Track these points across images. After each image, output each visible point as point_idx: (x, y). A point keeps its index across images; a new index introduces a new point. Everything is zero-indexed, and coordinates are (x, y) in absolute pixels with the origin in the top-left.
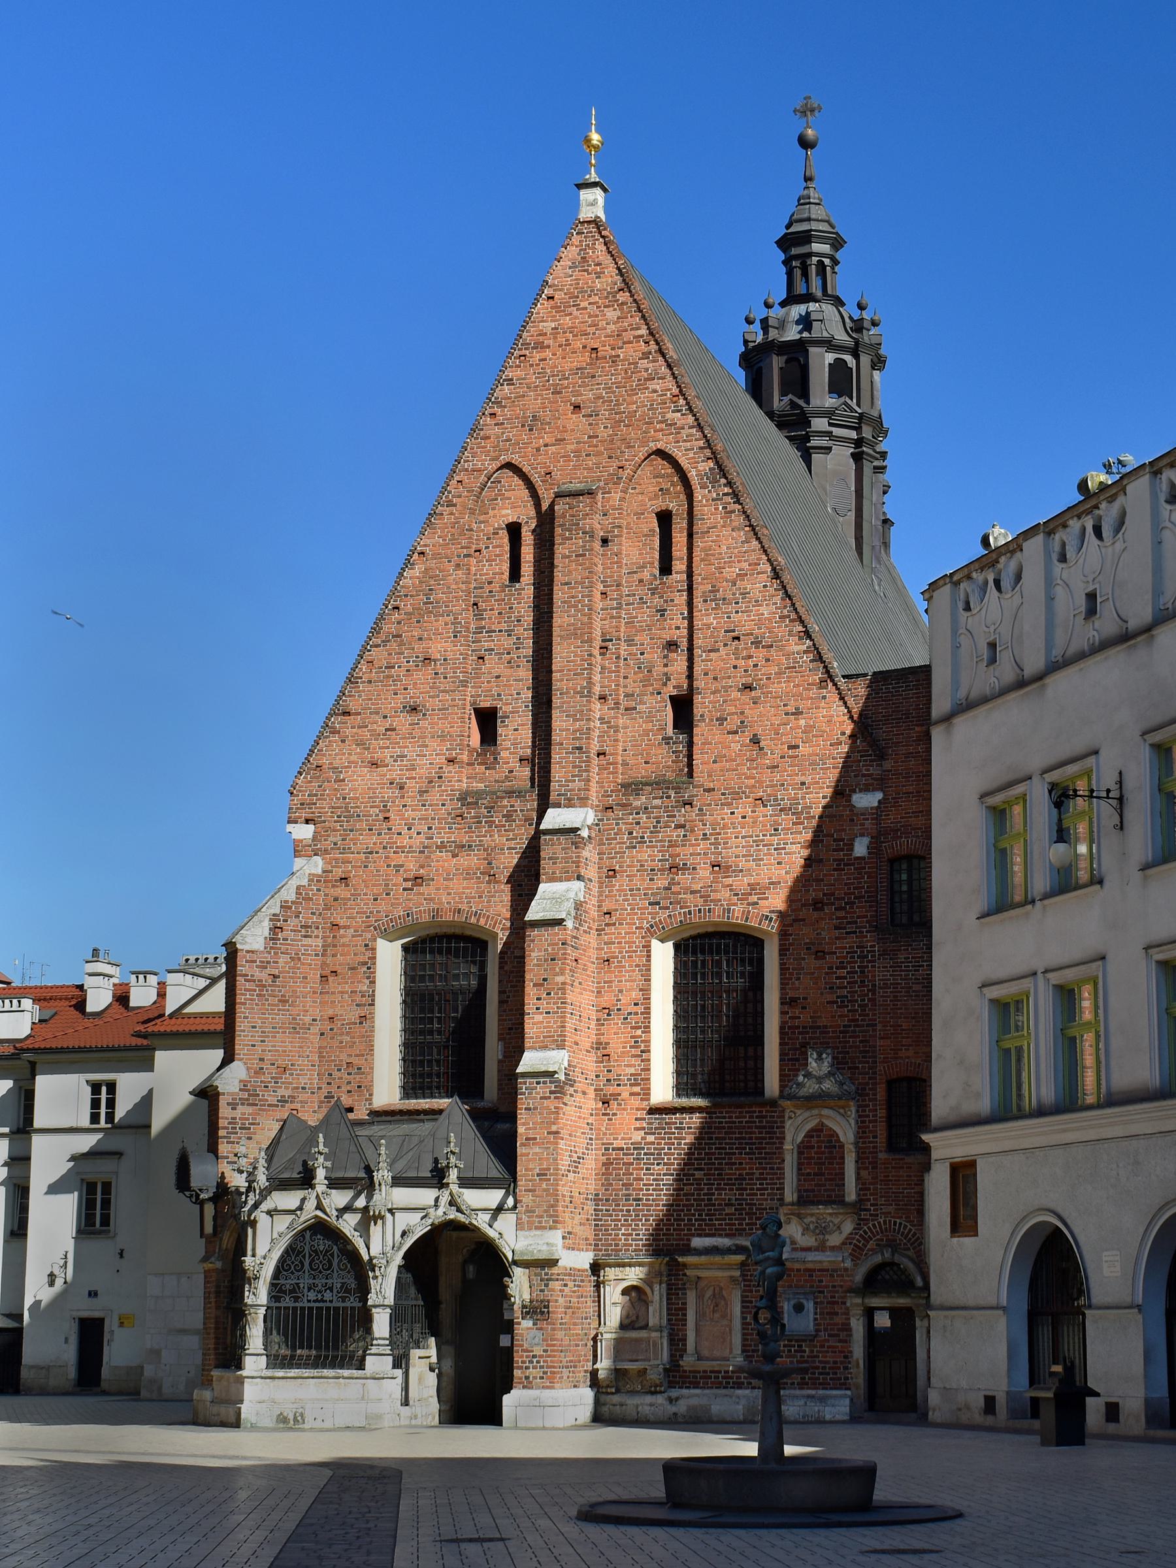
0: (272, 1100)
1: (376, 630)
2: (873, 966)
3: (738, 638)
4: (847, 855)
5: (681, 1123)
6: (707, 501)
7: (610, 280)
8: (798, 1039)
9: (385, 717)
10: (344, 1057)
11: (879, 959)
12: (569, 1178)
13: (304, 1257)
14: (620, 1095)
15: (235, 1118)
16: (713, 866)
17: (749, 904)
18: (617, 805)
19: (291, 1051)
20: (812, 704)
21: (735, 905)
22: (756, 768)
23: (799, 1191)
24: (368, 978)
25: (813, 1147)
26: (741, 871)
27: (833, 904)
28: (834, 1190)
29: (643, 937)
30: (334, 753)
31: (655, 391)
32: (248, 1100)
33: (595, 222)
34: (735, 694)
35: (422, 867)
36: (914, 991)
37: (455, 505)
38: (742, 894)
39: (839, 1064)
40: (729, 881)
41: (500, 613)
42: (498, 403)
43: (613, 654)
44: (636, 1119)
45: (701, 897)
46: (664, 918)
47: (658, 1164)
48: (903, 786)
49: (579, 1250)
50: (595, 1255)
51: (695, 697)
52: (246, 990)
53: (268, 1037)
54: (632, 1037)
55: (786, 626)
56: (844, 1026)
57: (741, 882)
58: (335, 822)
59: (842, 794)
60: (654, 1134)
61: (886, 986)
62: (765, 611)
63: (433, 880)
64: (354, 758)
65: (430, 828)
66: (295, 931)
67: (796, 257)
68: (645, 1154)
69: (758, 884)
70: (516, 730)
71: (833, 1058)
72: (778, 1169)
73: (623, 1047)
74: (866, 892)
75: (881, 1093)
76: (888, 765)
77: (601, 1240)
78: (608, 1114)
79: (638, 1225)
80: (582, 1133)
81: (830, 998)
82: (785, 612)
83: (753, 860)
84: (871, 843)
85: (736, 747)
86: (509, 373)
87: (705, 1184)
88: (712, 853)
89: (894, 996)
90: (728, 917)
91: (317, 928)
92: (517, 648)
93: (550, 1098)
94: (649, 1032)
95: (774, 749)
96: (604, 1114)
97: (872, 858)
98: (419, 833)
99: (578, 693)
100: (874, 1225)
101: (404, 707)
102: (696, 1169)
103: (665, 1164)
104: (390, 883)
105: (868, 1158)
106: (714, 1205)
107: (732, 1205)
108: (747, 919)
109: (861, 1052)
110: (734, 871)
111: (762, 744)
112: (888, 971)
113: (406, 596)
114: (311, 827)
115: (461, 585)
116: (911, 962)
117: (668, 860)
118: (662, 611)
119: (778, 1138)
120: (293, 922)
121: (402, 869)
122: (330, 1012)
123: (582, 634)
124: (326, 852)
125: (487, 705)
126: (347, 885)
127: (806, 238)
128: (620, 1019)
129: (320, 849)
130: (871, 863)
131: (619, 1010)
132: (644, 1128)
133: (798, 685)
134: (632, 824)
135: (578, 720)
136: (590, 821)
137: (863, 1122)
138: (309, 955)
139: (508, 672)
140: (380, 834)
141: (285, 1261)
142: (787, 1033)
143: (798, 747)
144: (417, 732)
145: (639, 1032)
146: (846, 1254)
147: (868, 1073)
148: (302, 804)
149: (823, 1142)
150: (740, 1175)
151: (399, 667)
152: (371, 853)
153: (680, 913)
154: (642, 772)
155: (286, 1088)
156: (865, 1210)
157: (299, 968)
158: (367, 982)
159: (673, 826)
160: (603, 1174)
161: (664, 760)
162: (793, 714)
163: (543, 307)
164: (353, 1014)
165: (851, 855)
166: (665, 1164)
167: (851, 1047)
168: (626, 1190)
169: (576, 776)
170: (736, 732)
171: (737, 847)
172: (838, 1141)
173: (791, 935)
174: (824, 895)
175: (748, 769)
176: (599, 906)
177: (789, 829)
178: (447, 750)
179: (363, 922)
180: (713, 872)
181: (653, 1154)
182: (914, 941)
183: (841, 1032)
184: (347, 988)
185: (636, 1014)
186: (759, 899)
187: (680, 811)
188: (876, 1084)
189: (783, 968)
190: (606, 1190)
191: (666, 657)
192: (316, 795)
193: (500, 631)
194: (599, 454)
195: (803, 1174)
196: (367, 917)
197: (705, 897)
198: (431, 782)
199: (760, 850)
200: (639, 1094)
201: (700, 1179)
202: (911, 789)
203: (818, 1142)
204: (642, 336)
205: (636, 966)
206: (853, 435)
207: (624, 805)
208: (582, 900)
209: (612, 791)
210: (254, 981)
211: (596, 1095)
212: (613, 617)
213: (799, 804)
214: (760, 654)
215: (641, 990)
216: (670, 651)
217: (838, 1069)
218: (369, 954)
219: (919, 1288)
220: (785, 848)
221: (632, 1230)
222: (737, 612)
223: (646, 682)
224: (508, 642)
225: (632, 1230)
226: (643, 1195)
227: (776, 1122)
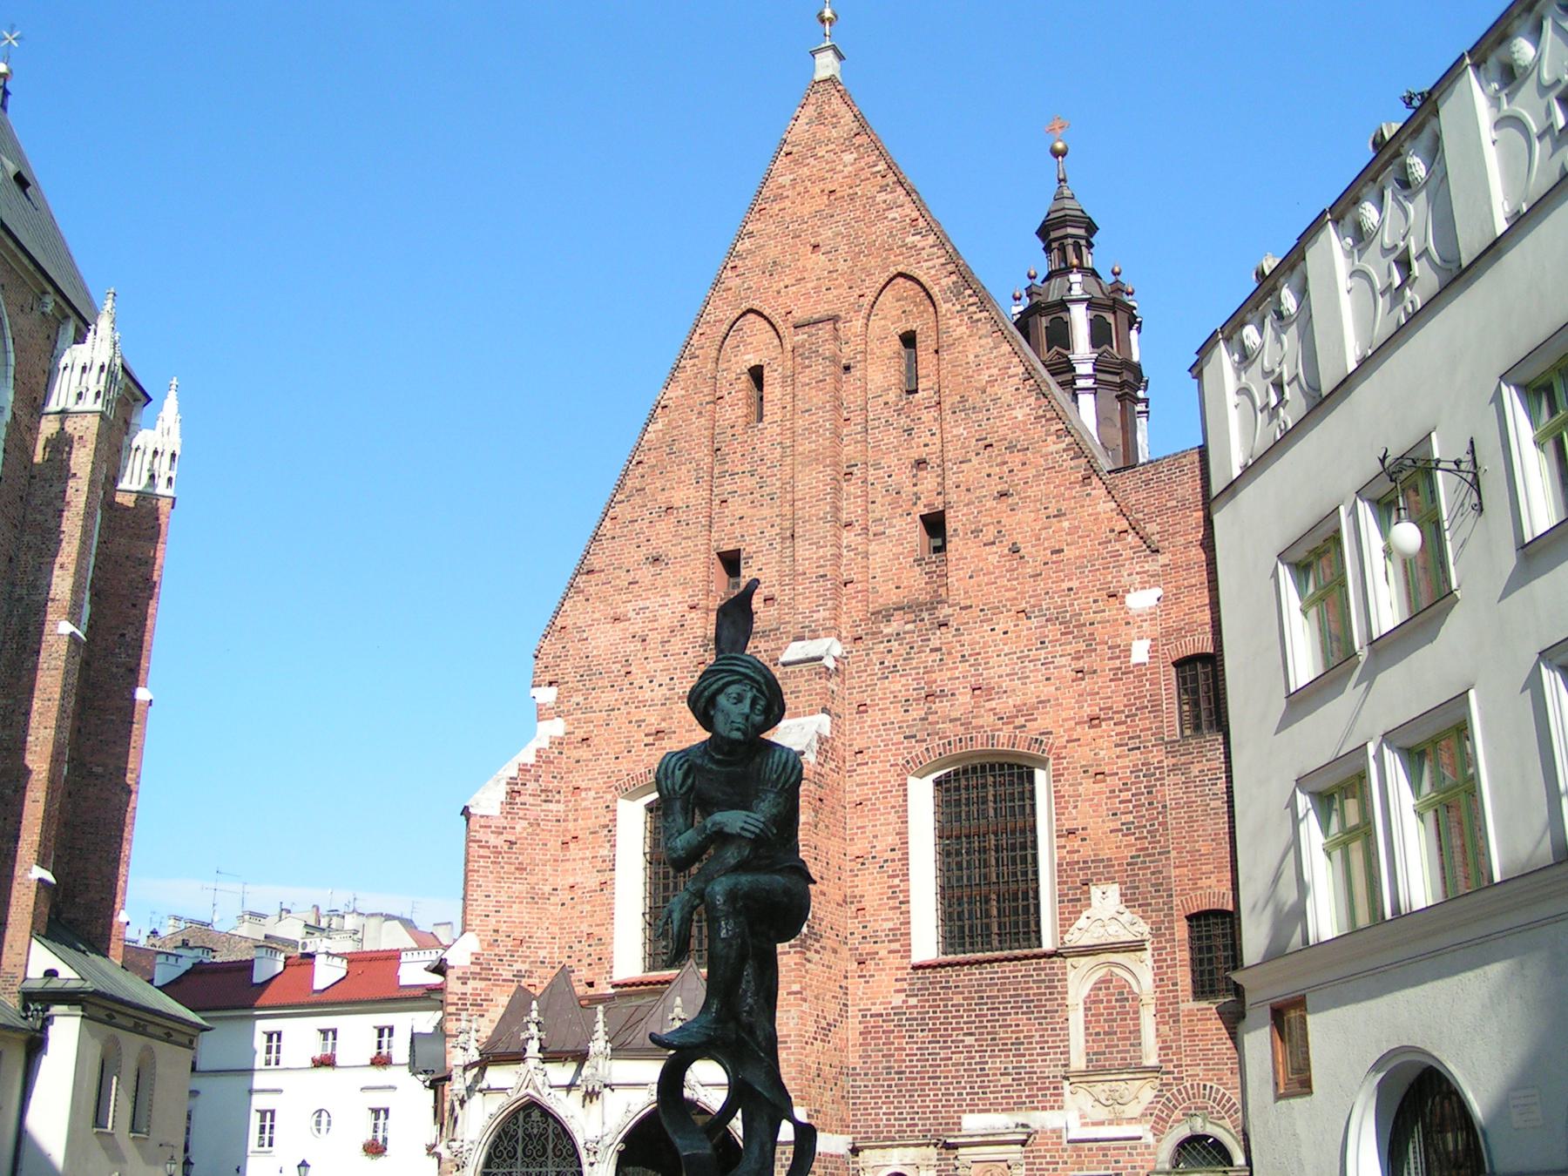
0: (507, 975)
1: (620, 486)
2: (1161, 785)
3: (991, 445)
4: (1125, 662)
5: (947, 982)
6: (951, 314)
7: (846, 128)
8: (1078, 876)
9: (628, 571)
10: (585, 928)
11: (1169, 775)
12: (815, 1047)
13: (517, 1141)
14: (877, 953)
15: (466, 994)
16: (974, 690)
17: (1015, 728)
18: (867, 634)
19: (528, 923)
20: (1075, 503)
21: (1001, 730)
22: (1017, 579)
23: (1088, 1054)
24: (609, 841)
25: (1102, 1002)
26: (1005, 692)
27: (1112, 719)
28: (1128, 1051)
29: (898, 775)
30: (576, 613)
31: (894, 219)
32: (480, 974)
33: (830, 80)
34: (990, 503)
35: (664, 720)
36: (1212, 809)
37: (698, 357)
38: (1007, 718)
39: (1128, 900)
40: (993, 704)
41: (743, 455)
42: (739, 256)
43: (859, 478)
44: (896, 980)
45: (962, 725)
46: (922, 752)
47: (922, 1031)
48: (1184, 580)
49: (830, 1132)
50: (854, 1139)
51: (946, 512)
52: (480, 857)
53: (503, 907)
54: (889, 887)
55: (1042, 426)
56: (1132, 857)
57: (1006, 704)
58: (578, 681)
59: (1115, 596)
60: (917, 995)
61: (1178, 807)
62: (1019, 414)
63: (675, 732)
64: (597, 615)
65: (672, 679)
66: (534, 795)
67: (1055, 240)
68: (907, 1020)
69: (1025, 705)
70: (761, 569)
71: (1122, 895)
72: (1061, 1029)
73: (880, 899)
74: (1148, 701)
75: (1182, 930)
76: (1163, 559)
77: (859, 1121)
78: (865, 976)
79: (900, 1102)
80: (833, 997)
81: (1112, 826)
82: (1041, 412)
83: (1019, 679)
84: (1151, 646)
85: (994, 559)
86: (750, 227)
87: (976, 1051)
88: (972, 676)
89: (1189, 817)
90: (993, 745)
91: (559, 792)
92: (761, 487)
93: (789, 953)
94: (908, 880)
95: (1034, 555)
96: (859, 977)
97: (1154, 663)
98: (660, 685)
99: (821, 519)
100: (1179, 1090)
101: (647, 559)
102: (965, 1034)
103: (930, 1030)
104: (632, 740)
105: (1168, 1010)
106: (988, 1075)
107: (1008, 1074)
108: (1014, 744)
109: (1152, 885)
110: (998, 693)
111: (1022, 552)
112: (1181, 788)
113: (650, 450)
114: (554, 690)
115: (703, 432)
116: (1207, 775)
117: (923, 688)
118: (909, 431)
119: (1059, 993)
120: (531, 786)
121: (643, 724)
122: (571, 881)
123: (824, 458)
124: (569, 714)
125: (731, 547)
126: (589, 746)
127: (1062, 222)
128: (875, 868)
129: (563, 712)
130: (1152, 668)
131: (874, 857)
132: (905, 990)
133: (1059, 486)
134: (883, 653)
135: (822, 547)
136: (838, 649)
137: (1161, 967)
138: (549, 820)
139: (750, 512)
140: (621, 690)
141: (497, 1147)
142: (1066, 871)
143: (1063, 551)
144: (659, 583)
145: (897, 881)
146: (1148, 1127)
147: (1162, 910)
148: (546, 667)
149: (1113, 994)
150: (1016, 1038)
151: (642, 520)
152: (613, 710)
153: (938, 745)
154: (894, 597)
155: (524, 962)
156: (1168, 1073)
157: (538, 835)
158: (608, 845)
159: (928, 650)
160: (861, 1045)
161: (915, 582)
162: (1054, 516)
163: (783, 161)
164: (593, 881)
165: (1129, 662)
166: (930, 1030)
167: (1140, 881)
168: (887, 1062)
169: (821, 605)
170: (994, 543)
171: (1000, 666)
172: (1131, 992)
173: (1065, 758)
174: (1100, 710)
175: (1008, 580)
176: (850, 746)
177: (1057, 641)
178: (689, 597)
179: (604, 783)
180: (973, 696)
181: (916, 1019)
182: (1210, 750)
183: (1128, 864)
184: (588, 854)
185: (893, 860)
186: (1026, 721)
187: (935, 634)
188: (1172, 921)
189: (1059, 796)
190: (864, 1063)
191: (914, 476)
192: (560, 657)
193: (743, 473)
194: (841, 285)
195: (1091, 1034)
196: (609, 777)
197: (966, 724)
198: (673, 631)
199: (1025, 667)
200: (899, 951)
201: (970, 1046)
202: (1193, 581)
203: (1107, 995)
204: (879, 172)
205: (893, 807)
206: (1117, 379)
207: (874, 633)
208: (828, 735)
209: (861, 620)
210: (489, 847)
211: (851, 955)
212: (859, 442)
213: (1067, 611)
214: (1015, 460)
215: (897, 834)
216: (919, 469)
217: (1127, 907)
218: (610, 816)
219: (1239, 1166)
220: (1053, 662)
221: (895, 1108)
222: (988, 419)
223: (894, 505)
224: (751, 483)
225: (895, 1108)
226: (906, 1067)
227: (1056, 975)
